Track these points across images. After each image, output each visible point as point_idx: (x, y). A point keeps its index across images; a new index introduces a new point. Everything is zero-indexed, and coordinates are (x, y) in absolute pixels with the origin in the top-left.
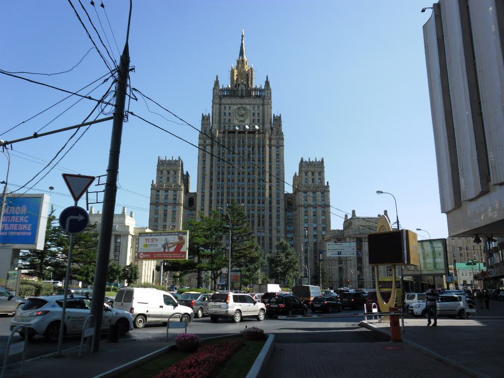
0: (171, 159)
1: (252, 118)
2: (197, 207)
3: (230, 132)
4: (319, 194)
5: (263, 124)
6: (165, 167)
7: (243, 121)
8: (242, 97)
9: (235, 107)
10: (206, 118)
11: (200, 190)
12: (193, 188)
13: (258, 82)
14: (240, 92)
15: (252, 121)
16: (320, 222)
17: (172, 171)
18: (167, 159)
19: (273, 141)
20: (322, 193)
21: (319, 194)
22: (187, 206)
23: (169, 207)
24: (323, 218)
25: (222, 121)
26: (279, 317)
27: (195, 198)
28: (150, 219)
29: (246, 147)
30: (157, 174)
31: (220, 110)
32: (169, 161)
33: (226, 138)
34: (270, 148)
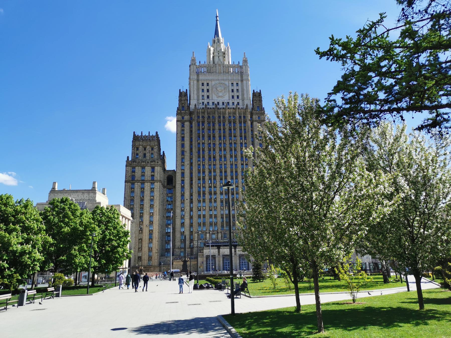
0: (147, 135)
1: (231, 94)
2: (177, 184)
6: (141, 143)
7: (222, 97)
10: (183, 94)
11: (180, 167)
12: (171, 164)
15: (231, 97)
18: (144, 135)
19: (254, 116)
22: (166, 184)
27: (174, 177)
28: (125, 198)
30: (132, 150)
32: (146, 136)
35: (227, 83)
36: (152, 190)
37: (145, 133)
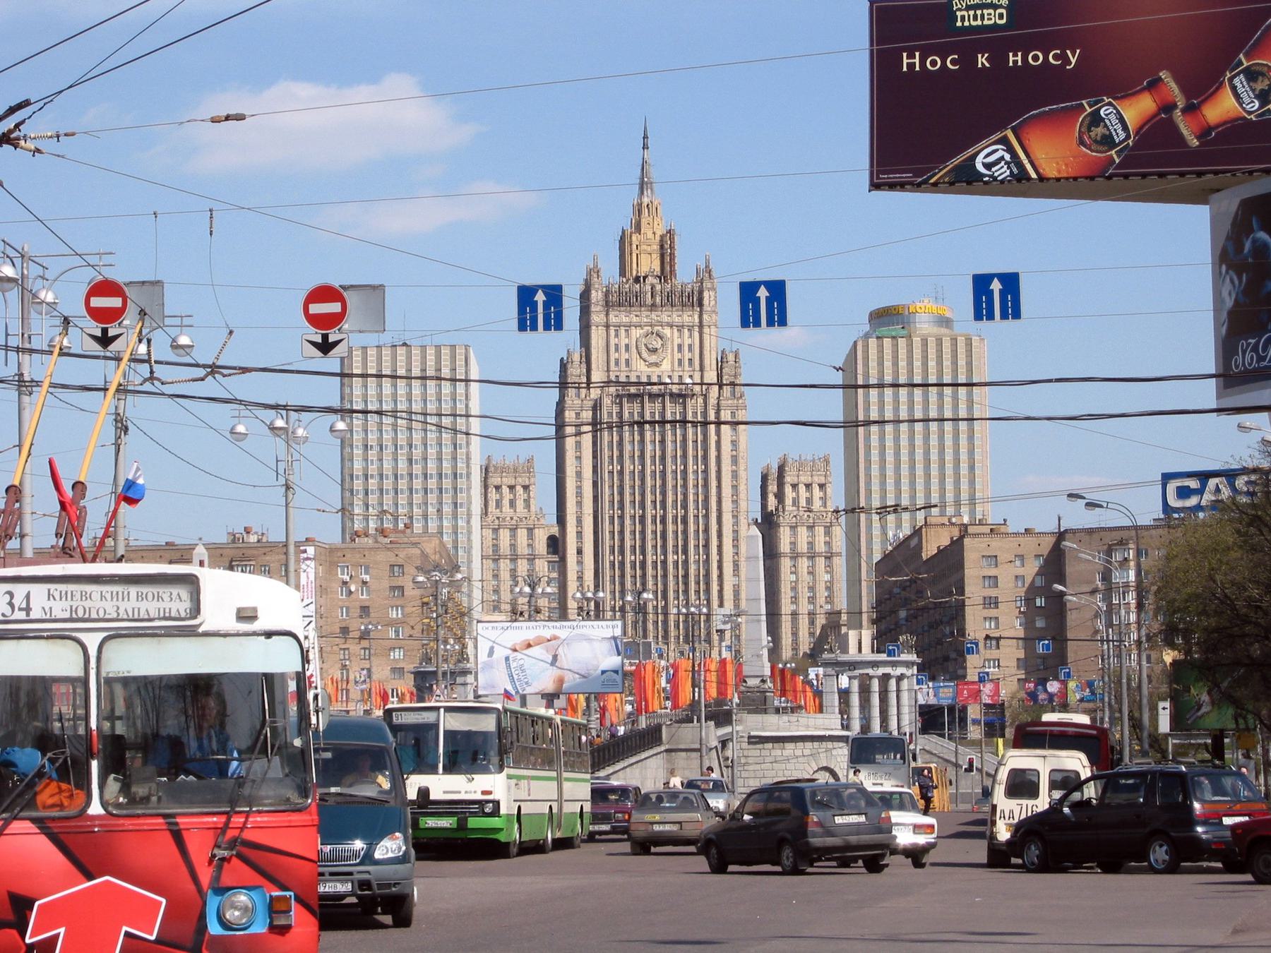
1: (677, 356)
7: (657, 365)
8: (653, 307)
19: (722, 413)
26: (731, 868)
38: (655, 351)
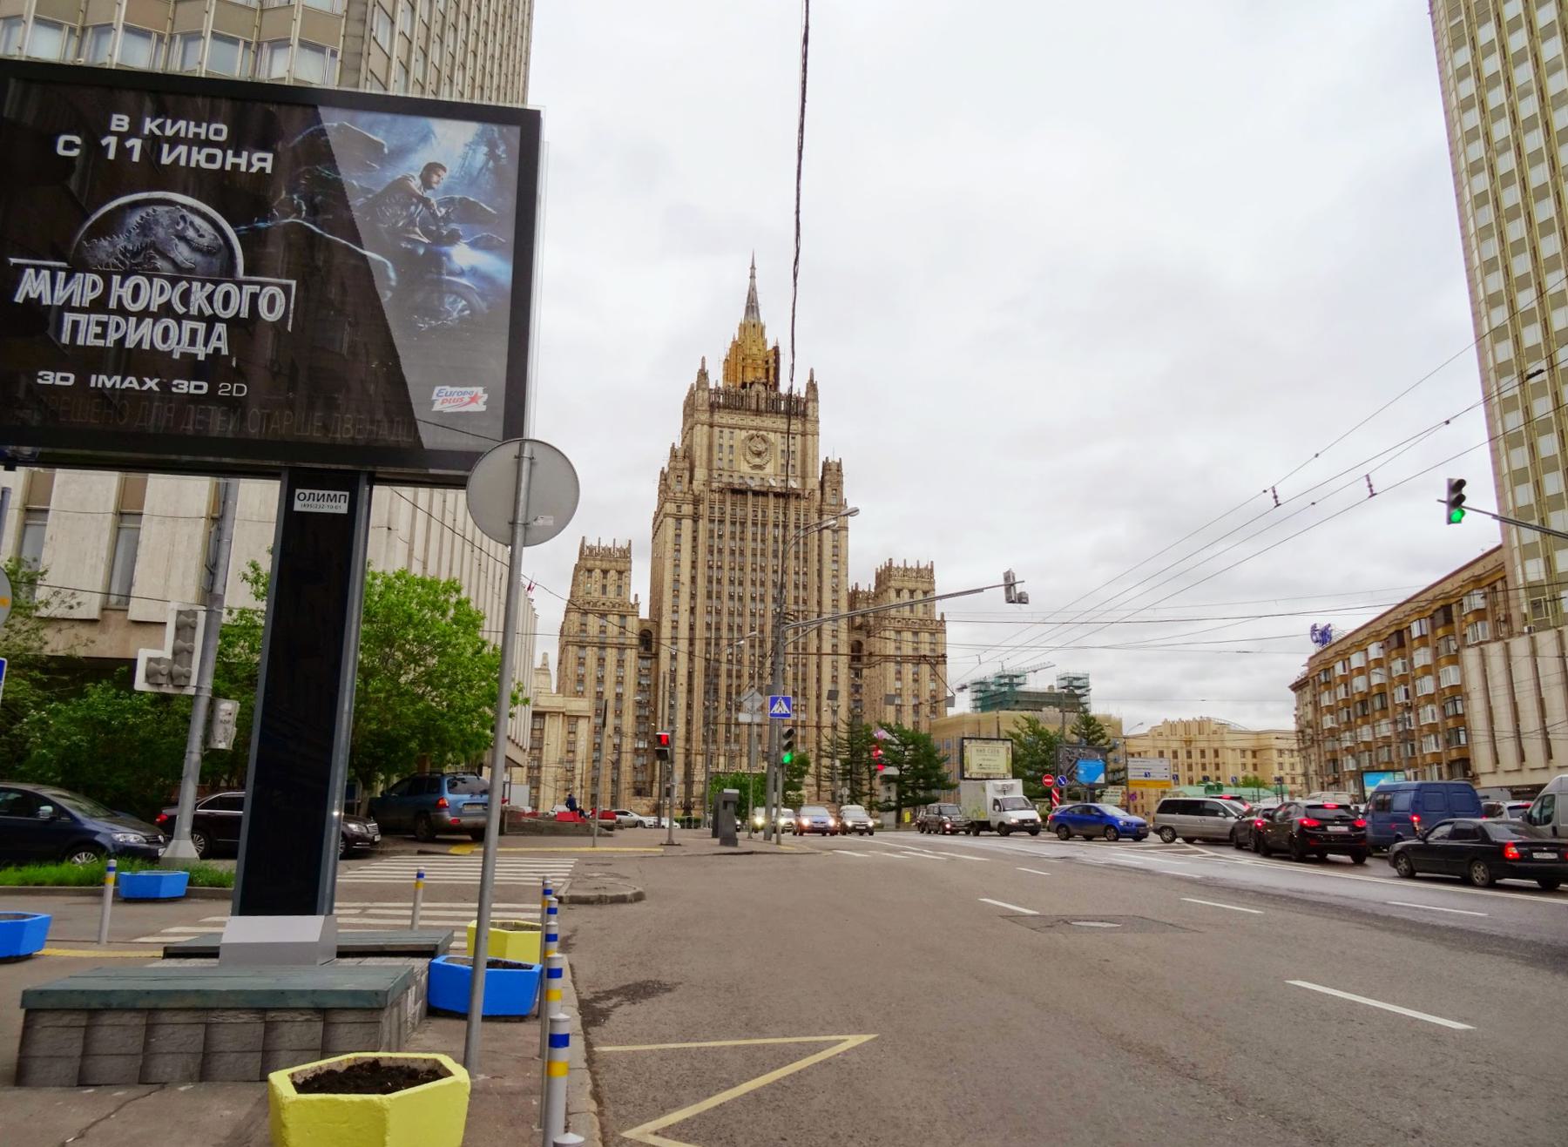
3: (735, 491)
4: (925, 637)
5: (804, 477)
7: (760, 467)
8: (758, 412)
9: (744, 434)
13: (791, 382)
14: (754, 401)
16: (926, 695)
17: (612, 573)
20: (932, 634)
21: (925, 637)
23: (609, 650)
24: (933, 686)
25: (716, 464)
29: (770, 526)
31: (710, 437)
33: (728, 504)
34: (820, 531)
35: (771, 436)
36: (620, 663)
37: (607, 542)
38: (759, 454)
